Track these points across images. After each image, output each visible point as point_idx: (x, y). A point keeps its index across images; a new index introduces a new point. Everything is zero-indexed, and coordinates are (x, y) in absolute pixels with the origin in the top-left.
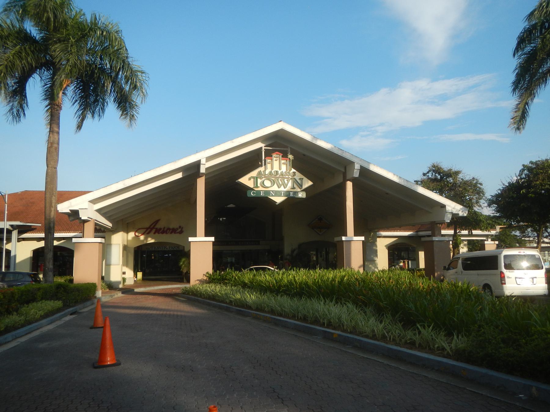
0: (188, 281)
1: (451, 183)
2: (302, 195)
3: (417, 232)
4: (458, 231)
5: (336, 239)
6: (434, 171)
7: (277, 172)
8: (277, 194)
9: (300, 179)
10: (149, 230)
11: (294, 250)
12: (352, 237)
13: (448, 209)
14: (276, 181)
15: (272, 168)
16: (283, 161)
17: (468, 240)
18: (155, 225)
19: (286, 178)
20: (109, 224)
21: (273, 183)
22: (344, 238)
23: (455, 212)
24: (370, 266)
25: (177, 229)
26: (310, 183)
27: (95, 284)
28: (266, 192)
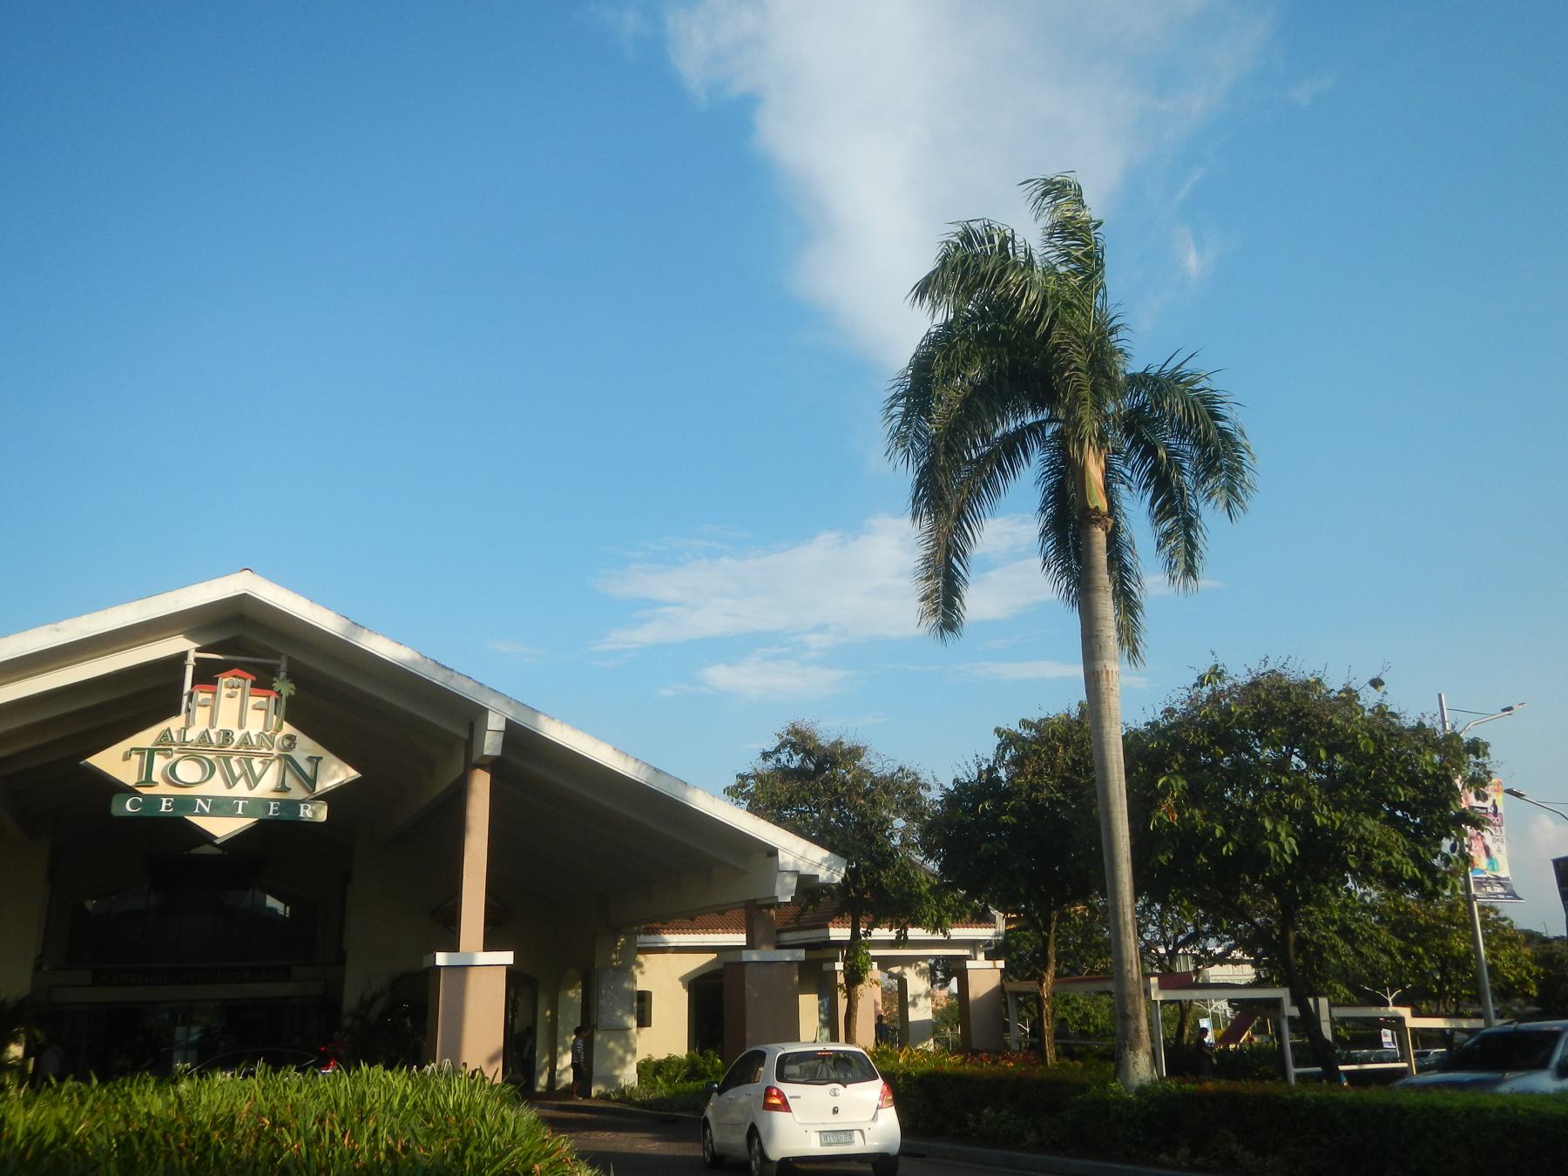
1: (844, 784)
4: (862, 930)
5: (426, 964)
6: (793, 745)
7: (227, 735)
8: (222, 807)
9: (310, 759)
11: (374, 999)
12: (471, 956)
13: (786, 859)
14: (225, 764)
15: (212, 725)
16: (253, 701)
17: (937, 958)
23: (805, 869)
24: (611, 1045)
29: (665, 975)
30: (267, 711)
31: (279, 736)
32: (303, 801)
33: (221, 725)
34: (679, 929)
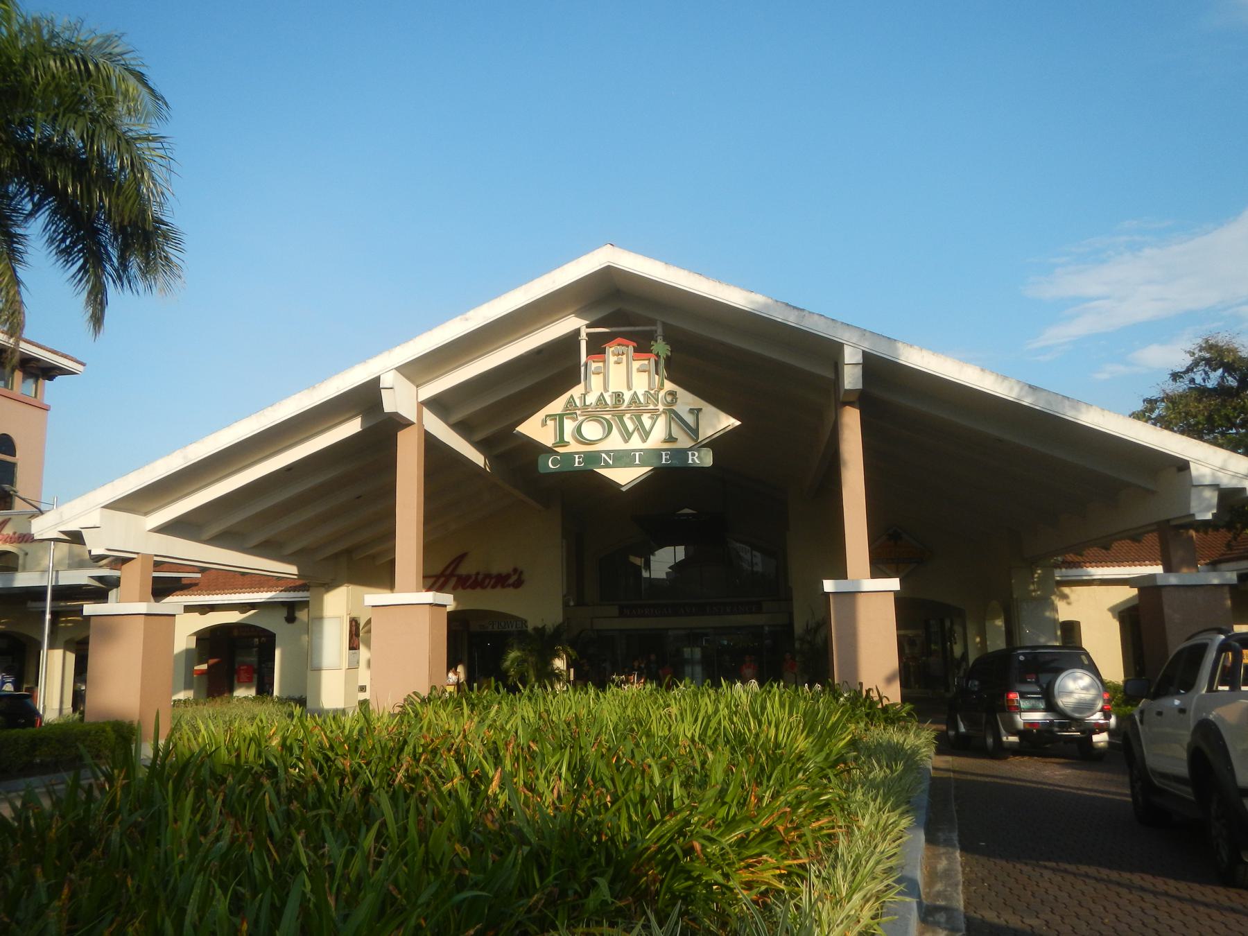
2: (704, 459)
6: (1208, 362)
7: (618, 396)
8: (623, 459)
9: (691, 411)
10: (442, 579)
12: (857, 582)
14: (623, 422)
16: (636, 365)
18: (455, 569)
19: (649, 411)
22: (829, 586)
23: (1227, 481)
25: (508, 576)
26: (728, 422)
27: (131, 724)
29: (1093, 608)
31: (662, 394)
32: (691, 449)
33: (612, 389)
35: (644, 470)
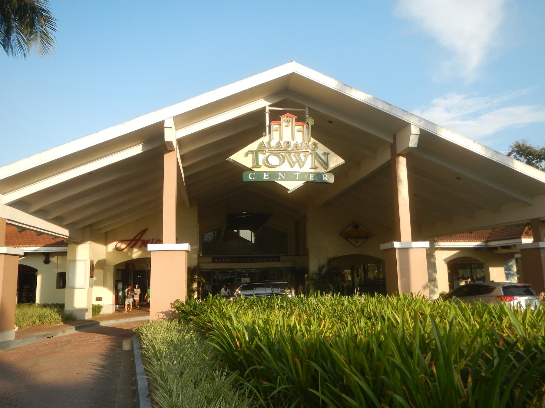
0: (149, 314)
2: (330, 179)
3: (486, 242)
5: (383, 246)
8: (290, 176)
9: (324, 154)
10: (134, 242)
11: (323, 267)
15: (281, 138)
16: (297, 128)
19: (303, 152)
20: (64, 232)
21: (282, 160)
28: (271, 174)
30: (303, 132)
31: (310, 143)
32: (323, 173)
34: (443, 240)
35: (300, 183)
